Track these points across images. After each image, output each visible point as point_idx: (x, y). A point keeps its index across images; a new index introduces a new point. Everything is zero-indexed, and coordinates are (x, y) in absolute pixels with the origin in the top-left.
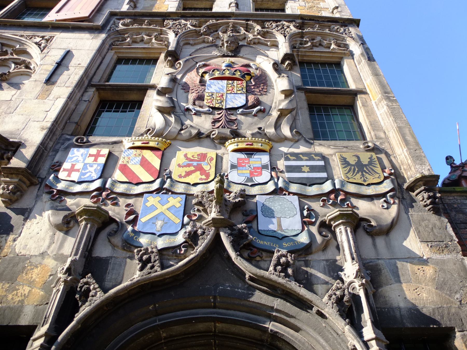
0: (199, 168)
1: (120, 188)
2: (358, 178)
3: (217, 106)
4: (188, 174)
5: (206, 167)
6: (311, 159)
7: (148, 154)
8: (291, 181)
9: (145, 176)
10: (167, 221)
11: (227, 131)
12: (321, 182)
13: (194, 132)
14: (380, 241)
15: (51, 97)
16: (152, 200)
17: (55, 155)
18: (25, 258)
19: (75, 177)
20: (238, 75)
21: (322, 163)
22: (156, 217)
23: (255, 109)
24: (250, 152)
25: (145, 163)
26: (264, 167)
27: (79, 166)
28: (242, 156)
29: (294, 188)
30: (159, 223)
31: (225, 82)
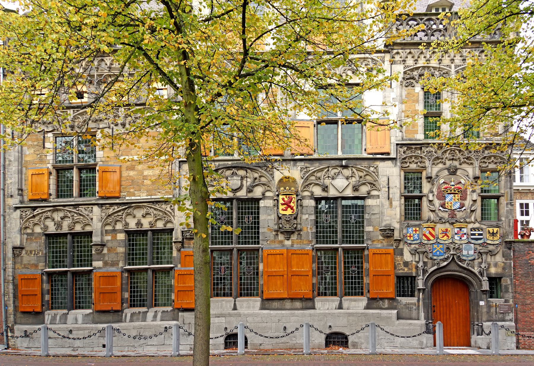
0: (446, 234)
1: (426, 242)
2: (491, 238)
3: (450, 208)
4: (443, 237)
5: (448, 234)
6: (479, 231)
7: (431, 230)
8: (472, 239)
9: (432, 238)
10: (440, 252)
11: (454, 221)
12: (481, 239)
13: (444, 221)
14: (493, 257)
15: (393, 206)
16: (435, 246)
17: (403, 230)
18: (408, 262)
19: (412, 239)
20: (456, 192)
21: (482, 232)
22: (437, 251)
23: (463, 209)
24: (461, 229)
25: (430, 233)
26: (465, 234)
27: (412, 235)
28: (458, 229)
29: (473, 241)
30: (438, 253)
31: (452, 195)
